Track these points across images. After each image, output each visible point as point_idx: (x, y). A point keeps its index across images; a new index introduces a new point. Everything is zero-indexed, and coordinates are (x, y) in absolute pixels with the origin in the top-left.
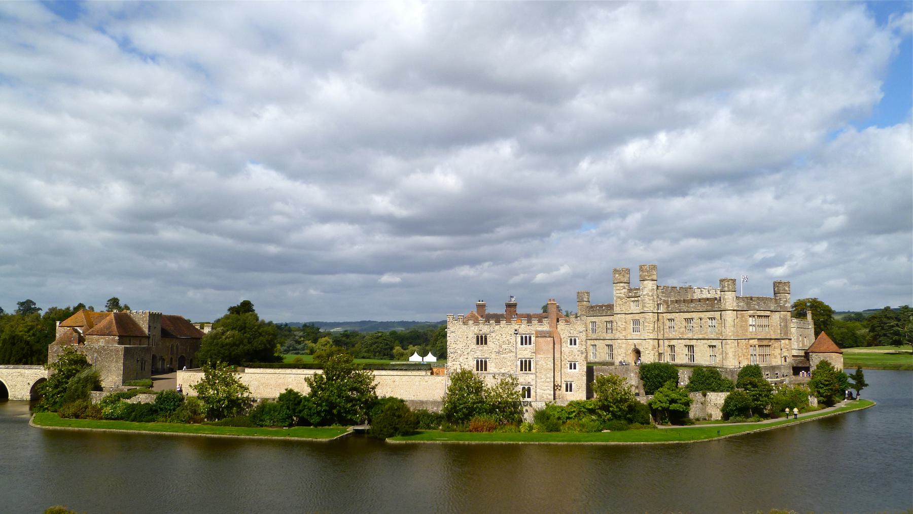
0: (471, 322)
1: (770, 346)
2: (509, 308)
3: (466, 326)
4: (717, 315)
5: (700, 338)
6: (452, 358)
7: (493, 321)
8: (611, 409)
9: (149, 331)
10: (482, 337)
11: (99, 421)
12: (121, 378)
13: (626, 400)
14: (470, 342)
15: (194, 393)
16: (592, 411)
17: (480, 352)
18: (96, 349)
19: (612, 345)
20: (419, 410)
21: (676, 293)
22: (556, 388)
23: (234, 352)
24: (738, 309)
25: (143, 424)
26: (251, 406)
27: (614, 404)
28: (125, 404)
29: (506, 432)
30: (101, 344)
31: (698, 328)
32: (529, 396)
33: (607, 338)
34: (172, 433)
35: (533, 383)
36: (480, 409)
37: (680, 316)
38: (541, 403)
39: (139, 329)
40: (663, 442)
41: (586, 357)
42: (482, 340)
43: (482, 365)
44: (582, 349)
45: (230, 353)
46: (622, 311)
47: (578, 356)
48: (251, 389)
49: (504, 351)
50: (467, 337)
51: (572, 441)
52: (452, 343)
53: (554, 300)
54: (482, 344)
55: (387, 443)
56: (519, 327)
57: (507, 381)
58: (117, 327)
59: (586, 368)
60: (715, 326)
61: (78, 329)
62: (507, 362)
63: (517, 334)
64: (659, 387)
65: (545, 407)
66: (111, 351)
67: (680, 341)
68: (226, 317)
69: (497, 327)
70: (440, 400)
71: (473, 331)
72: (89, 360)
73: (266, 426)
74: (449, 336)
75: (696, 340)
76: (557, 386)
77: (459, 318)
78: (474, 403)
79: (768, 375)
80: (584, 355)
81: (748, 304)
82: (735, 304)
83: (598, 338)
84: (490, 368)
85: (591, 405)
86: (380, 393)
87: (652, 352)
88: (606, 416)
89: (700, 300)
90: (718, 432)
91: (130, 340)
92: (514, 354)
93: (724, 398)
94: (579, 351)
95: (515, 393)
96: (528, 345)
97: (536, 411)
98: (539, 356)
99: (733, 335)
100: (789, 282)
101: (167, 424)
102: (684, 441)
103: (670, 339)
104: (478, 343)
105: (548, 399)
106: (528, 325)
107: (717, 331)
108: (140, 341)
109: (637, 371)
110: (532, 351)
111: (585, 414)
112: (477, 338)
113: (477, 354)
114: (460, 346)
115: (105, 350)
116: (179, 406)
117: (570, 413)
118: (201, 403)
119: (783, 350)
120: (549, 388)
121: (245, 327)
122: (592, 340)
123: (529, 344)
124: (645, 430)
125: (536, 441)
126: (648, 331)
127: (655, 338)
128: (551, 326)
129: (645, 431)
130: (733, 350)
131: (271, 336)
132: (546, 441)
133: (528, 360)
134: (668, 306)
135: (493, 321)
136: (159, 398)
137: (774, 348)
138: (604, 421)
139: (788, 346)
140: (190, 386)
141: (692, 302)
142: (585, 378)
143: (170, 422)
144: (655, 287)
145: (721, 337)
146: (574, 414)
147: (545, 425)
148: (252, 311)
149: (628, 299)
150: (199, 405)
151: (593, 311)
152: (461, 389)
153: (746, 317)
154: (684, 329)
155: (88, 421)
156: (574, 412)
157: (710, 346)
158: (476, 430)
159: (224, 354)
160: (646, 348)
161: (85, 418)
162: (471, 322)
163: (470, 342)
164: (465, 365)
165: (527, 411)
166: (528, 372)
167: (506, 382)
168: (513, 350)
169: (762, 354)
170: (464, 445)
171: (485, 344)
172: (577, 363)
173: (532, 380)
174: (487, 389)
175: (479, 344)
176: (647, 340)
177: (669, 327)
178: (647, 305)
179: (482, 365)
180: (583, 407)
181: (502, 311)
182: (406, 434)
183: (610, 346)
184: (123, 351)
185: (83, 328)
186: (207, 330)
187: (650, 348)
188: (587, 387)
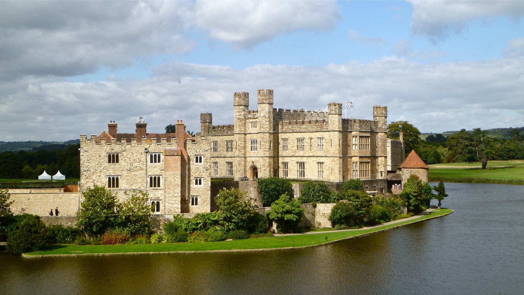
0: (103, 142)
2: (140, 129)
3: (99, 146)
4: (326, 135)
5: (310, 155)
6: (85, 176)
7: (125, 141)
10: (113, 155)
14: (102, 160)
17: (112, 170)
20: (54, 226)
31: (308, 147)
32: (158, 210)
33: (227, 156)
37: (293, 136)
42: (113, 158)
43: (114, 182)
44: (207, 166)
46: (241, 131)
47: (203, 172)
50: (100, 156)
52: (85, 162)
54: (113, 162)
55: (23, 257)
56: (149, 146)
59: (210, 183)
60: (323, 145)
64: (275, 200)
69: (128, 146)
71: (106, 150)
74: (82, 155)
75: (306, 158)
79: (367, 188)
83: (220, 156)
84: (121, 185)
86: (15, 210)
90: (326, 238)
92: (145, 172)
93: (331, 208)
94: (204, 168)
96: (157, 163)
98: (168, 173)
103: (284, 157)
104: (109, 162)
105: (175, 212)
106: (158, 145)
107: (325, 149)
109: (256, 186)
113: (109, 172)
114: (93, 164)
120: (177, 202)
123: (158, 162)
124: (262, 238)
125: (166, 251)
126: (265, 149)
128: (178, 146)
133: (157, 177)
135: (125, 141)
142: (209, 192)
145: (328, 155)
149: (247, 121)
157: (318, 163)
158: (109, 242)
160: (263, 165)
162: (103, 142)
163: (102, 160)
164: (98, 182)
166: (156, 188)
167: (137, 198)
168: (143, 168)
173: (161, 195)
176: (264, 158)
177: (283, 146)
179: (114, 182)
181: (132, 130)
182: (43, 248)
183: (230, 164)
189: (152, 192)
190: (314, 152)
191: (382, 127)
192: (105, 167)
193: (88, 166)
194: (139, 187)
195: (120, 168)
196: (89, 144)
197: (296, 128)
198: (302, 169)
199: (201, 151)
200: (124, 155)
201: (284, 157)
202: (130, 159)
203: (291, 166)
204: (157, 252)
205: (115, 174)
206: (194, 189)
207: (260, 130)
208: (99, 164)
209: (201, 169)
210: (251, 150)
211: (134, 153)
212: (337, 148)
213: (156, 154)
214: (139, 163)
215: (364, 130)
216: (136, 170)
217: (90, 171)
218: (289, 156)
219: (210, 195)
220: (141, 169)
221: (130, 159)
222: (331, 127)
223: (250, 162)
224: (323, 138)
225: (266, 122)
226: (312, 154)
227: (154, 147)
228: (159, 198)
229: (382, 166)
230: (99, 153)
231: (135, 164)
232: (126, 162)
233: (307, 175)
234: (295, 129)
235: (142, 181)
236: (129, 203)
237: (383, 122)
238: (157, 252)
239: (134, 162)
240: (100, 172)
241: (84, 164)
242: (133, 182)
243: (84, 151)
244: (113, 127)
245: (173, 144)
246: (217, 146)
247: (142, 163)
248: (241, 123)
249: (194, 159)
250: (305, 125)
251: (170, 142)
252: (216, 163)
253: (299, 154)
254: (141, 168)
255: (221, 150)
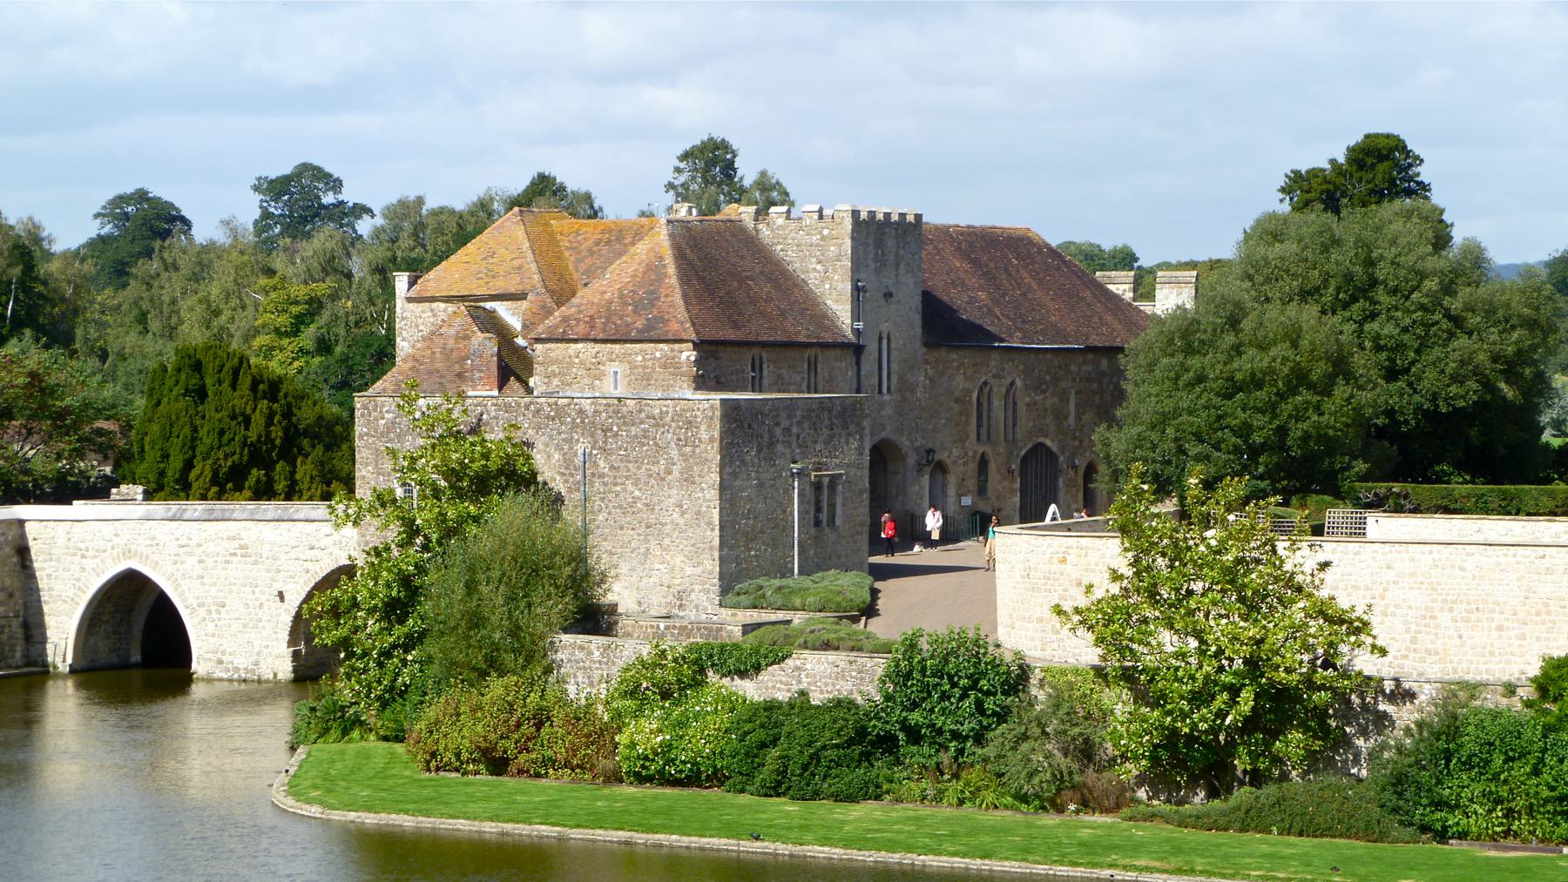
9: (856, 317)
11: (606, 791)
12: (711, 565)
15: (1083, 651)
18: (581, 412)
23: (1305, 425)
25: (828, 811)
26: (1382, 720)
28: (731, 702)
30: (608, 387)
34: (959, 862)
39: (810, 307)
41: (1429, 255)
45: (1282, 431)
48: (1382, 630)
58: (685, 296)
61: (503, 310)
66: (658, 422)
68: (1266, 232)
72: (547, 464)
73: (1463, 836)
91: (757, 366)
101: (946, 811)
108: (813, 366)
115: (628, 421)
116: (1002, 716)
118: (1119, 702)
121: (1373, 283)
131: (1515, 335)
136: (900, 676)
140: (1059, 611)
143: (961, 802)
148: (1409, 193)
150: (1106, 714)
155: (552, 785)
159: (1244, 431)
161: (538, 775)
184: (717, 424)
185: (524, 304)
186: (1171, 299)
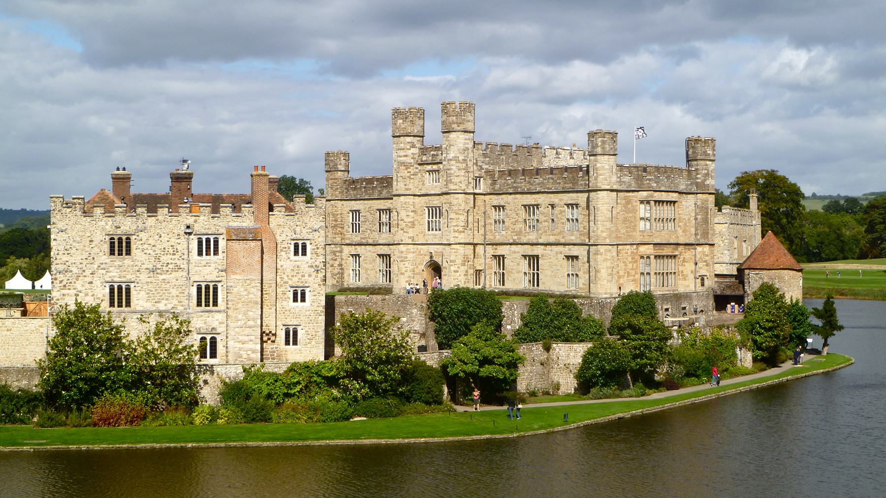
0: (98, 211)
1: (675, 256)
2: (178, 184)
3: (89, 219)
4: (582, 198)
6: (61, 282)
7: (144, 210)
8: (369, 377)
10: (120, 239)
13: (398, 360)
14: (96, 250)
16: (332, 382)
19: (389, 255)
21: (510, 157)
22: (265, 338)
24: (619, 188)
27: (375, 368)
29: (165, 425)
31: (546, 223)
32: (213, 355)
33: (380, 242)
35: (221, 329)
36: (114, 382)
38: (236, 368)
40: (461, 438)
44: (317, 263)
46: (407, 189)
47: (310, 276)
49: (165, 268)
51: (290, 440)
52: (61, 253)
53: (263, 168)
54: (120, 254)
56: (196, 221)
57: (167, 325)
60: (577, 220)
62: (171, 290)
63: (190, 234)
64: (460, 336)
65: (242, 376)
67: (514, 247)
69: (151, 221)
70: (34, 365)
71: (104, 229)
75: (542, 247)
76: (267, 335)
77: (75, 204)
78: (102, 371)
79: (667, 310)
80: (321, 275)
81: (639, 179)
82: (614, 179)
83: (364, 241)
84: (136, 302)
85: (331, 369)
87: (463, 268)
88: (358, 391)
89: (552, 170)
90: (565, 416)
92: (185, 274)
93: (582, 353)
94: (312, 266)
95: (184, 348)
97: (225, 383)
98: (233, 277)
99: (609, 236)
100: (713, 140)
102: (500, 433)
103: (496, 244)
104: (112, 253)
105: (250, 359)
107: (582, 229)
109: (424, 305)
110: (220, 268)
111: (320, 388)
112: (111, 243)
113: (111, 274)
114: (77, 257)
117: (289, 386)
119: (700, 265)
120: (253, 338)
122: (351, 245)
123: (214, 254)
124: (431, 415)
126: (456, 228)
127: (467, 241)
128: (256, 219)
129: (434, 417)
130: (609, 264)
132: (241, 440)
133: (211, 285)
134: (494, 182)
135: (144, 210)
137: (684, 261)
138: (355, 399)
139: (707, 258)
141: (537, 174)
144: (471, 145)
146: (298, 388)
147: (242, 410)
149: (420, 168)
151: (355, 189)
152: (77, 344)
153: (634, 204)
154: (522, 225)
156: (298, 383)
157: (568, 257)
158: (106, 421)
160: (451, 261)
162: (98, 211)
163: (96, 250)
164: (87, 295)
165: (206, 382)
166: (211, 308)
167: (166, 329)
168: (182, 266)
169: (662, 272)
170: (79, 452)
171: (127, 254)
172: (307, 290)
173: (220, 323)
174: (127, 344)
175: (114, 254)
176: (453, 246)
177: (495, 222)
178: (455, 180)
180: (316, 373)
181: (163, 186)
183: (386, 258)
187: (459, 261)
188: (326, 336)
189: (201, 316)
190: (558, 235)
191: (703, 182)
192: (102, 264)
193: (67, 261)
194: (172, 305)
195: (133, 266)
196: (69, 215)
197: (522, 184)
198: (534, 270)
199: (304, 231)
200: (141, 240)
201: (496, 244)
202: (153, 248)
203: (512, 264)
204: (202, 444)
205: (123, 280)
206: (290, 310)
207: (447, 188)
208: (90, 258)
209: (305, 268)
210: (429, 230)
211: (163, 235)
212: (606, 226)
213: (209, 236)
214: (174, 257)
215: (666, 187)
216: (168, 271)
217: (71, 271)
218: (507, 242)
219: (323, 324)
220: (178, 269)
221: (153, 248)
222: (594, 182)
223: (425, 255)
224: (577, 205)
225: (459, 170)
226: (556, 239)
227: (206, 223)
228: (216, 330)
229: (704, 265)
230: (89, 235)
231: (165, 259)
232: (145, 253)
233: (544, 283)
234: (519, 185)
235: (180, 293)
236: (148, 339)
237: (706, 172)
238: (202, 444)
239: (163, 253)
240: (92, 274)
241: (58, 257)
242: (161, 296)
243: (58, 231)
244: (121, 180)
245: (245, 216)
246: (359, 221)
247: (180, 257)
248: (408, 172)
249: (289, 248)
250: (541, 177)
251: (240, 211)
252: (356, 256)
253: (527, 238)
254: (177, 266)
255: (366, 229)
